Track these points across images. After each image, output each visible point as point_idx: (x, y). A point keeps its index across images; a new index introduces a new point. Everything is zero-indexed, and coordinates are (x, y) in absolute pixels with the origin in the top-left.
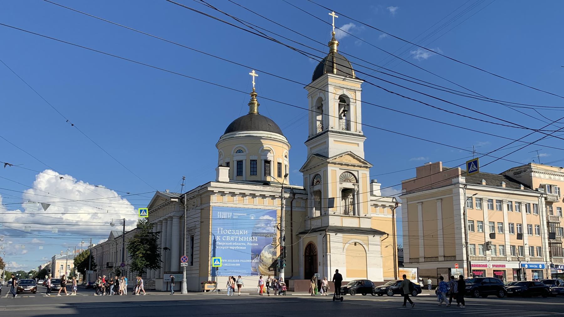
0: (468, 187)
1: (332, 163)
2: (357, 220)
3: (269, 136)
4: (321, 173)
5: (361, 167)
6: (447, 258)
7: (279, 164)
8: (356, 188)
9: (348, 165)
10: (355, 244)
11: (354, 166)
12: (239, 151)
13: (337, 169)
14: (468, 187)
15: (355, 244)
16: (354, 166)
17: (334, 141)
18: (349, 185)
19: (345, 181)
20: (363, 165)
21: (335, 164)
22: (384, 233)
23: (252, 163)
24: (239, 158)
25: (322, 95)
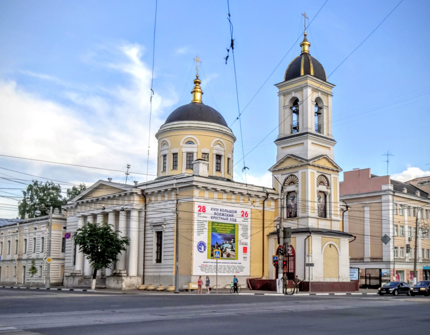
0: (396, 194)
1: (312, 165)
2: (328, 223)
3: (221, 129)
4: (299, 174)
5: (333, 170)
6: (374, 260)
7: (229, 159)
8: (329, 191)
9: (323, 168)
10: (330, 247)
11: (328, 169)
12: (190, 142)
13: (315, 172)
14: (396, 194)
15: (330, 247)
16: (328, 169)
17: (312, 143)
18: (323, 188)
19: (320, 184)
20: (335, 169)
21: (314, 166)
22: (351, 236)
23: (189, 155)
24: (190, 150)
25: (298, 95)
